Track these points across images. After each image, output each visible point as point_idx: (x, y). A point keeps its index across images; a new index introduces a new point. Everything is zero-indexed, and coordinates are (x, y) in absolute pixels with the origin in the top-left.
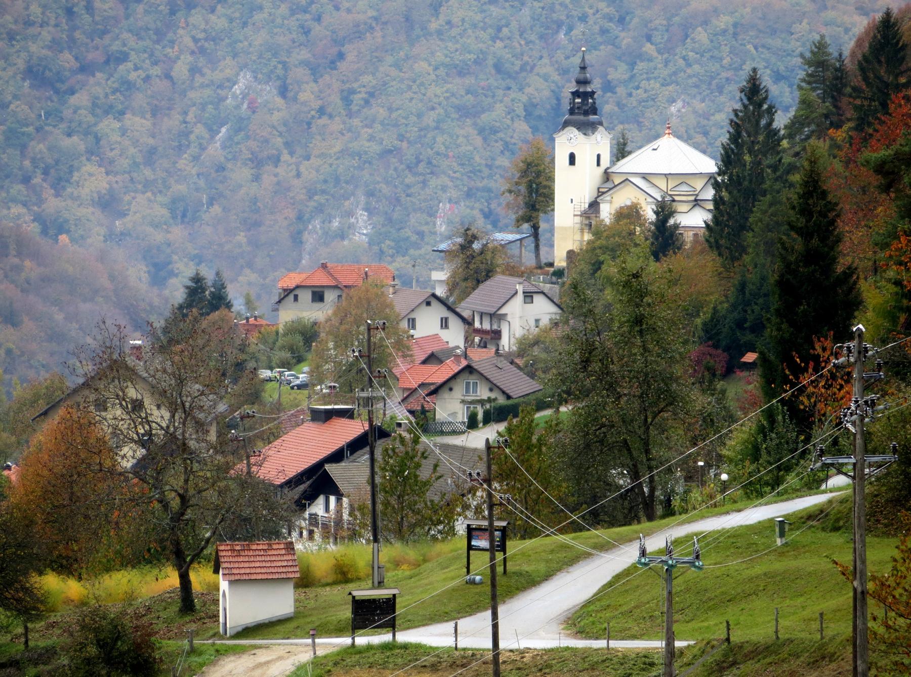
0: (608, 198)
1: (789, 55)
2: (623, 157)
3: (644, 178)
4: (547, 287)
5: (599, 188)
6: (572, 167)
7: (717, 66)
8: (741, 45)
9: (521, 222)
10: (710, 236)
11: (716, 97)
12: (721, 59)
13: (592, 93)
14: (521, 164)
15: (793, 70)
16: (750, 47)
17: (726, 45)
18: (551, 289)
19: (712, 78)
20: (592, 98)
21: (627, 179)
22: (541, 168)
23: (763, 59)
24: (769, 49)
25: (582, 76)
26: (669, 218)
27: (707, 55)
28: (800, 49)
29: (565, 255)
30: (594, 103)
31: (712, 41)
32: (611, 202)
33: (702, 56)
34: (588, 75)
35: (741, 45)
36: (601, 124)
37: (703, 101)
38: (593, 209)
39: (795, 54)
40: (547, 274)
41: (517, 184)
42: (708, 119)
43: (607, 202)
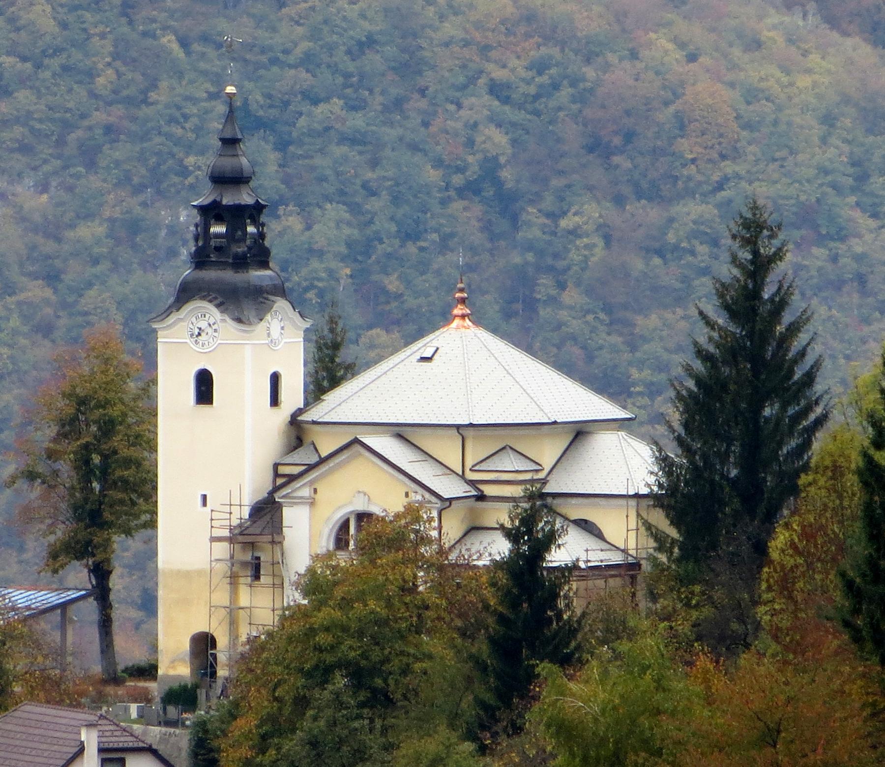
0: (306, 492)
1: (274, 61)
2: (335, 382)
3: (400, 437)
4: (154, 734)
5: (276, 466)
6: (275, 409)
7: (81, 92)
8: (145, 34)
9: (62, 559)
10: (856, 611)
11: (78, 176)
12: (91, 74)
13: (255, 211)
14: (61, 403)
15: (286, 104)
16: (169, 41)
17: (103, 36)
18: (164, 739)
19: (67, 126)
20: (255, 222)
21: (356, 441)
22: (115, 412)
23: (205, 73)
24: (219, 46)
25: (227, 164)
26: (547, 549)
27: (55, 63)
28: (305, 45)
29: (186, 645)
30: (262, 236)
31: (64, 26)
32: (312, 503)
33: (38, 66)
34: (244, 161)
35: (145, 34)
36: (280, 291)
37: (43, 187)
38: (261, 523)
39: (291, 59)
40: (144, 697)
41: (51, 455)
42: (59, 240)
43: (302, 501)
